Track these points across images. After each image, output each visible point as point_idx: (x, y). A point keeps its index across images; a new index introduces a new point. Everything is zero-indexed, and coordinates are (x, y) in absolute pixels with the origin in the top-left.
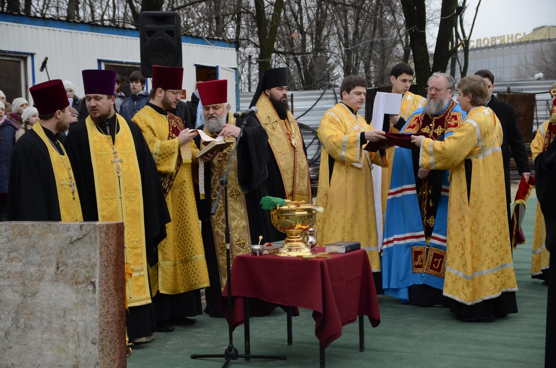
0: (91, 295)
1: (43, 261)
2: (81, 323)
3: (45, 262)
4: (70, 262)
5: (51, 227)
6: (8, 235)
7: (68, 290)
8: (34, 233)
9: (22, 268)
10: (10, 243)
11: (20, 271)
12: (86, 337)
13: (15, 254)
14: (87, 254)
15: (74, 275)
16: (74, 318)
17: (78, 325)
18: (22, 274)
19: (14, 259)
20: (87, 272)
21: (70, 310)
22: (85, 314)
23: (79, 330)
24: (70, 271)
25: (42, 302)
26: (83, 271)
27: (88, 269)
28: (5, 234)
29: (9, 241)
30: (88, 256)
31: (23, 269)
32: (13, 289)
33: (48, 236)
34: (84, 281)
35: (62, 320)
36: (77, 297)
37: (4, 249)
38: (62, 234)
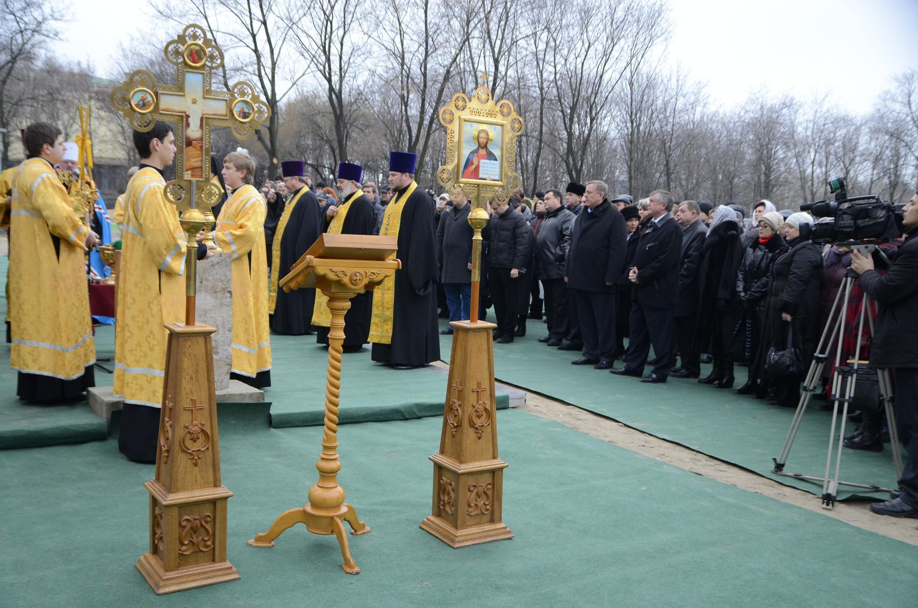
0: (228, 300)
2: (219, 319)
4: (210, 278)
7: (208, 297)
12: (223, 327)
15: (213, 287)
16: (213, 315)
17: (216, 320)
20: (224, 284)
21: (210, 310)
22: (223, 313)
23: (218, 323)
24: (210, 284)
26: (220, 284)
27: (224, 283)
34: (221, 291)
35: (203, 318)
36: (216, 302)
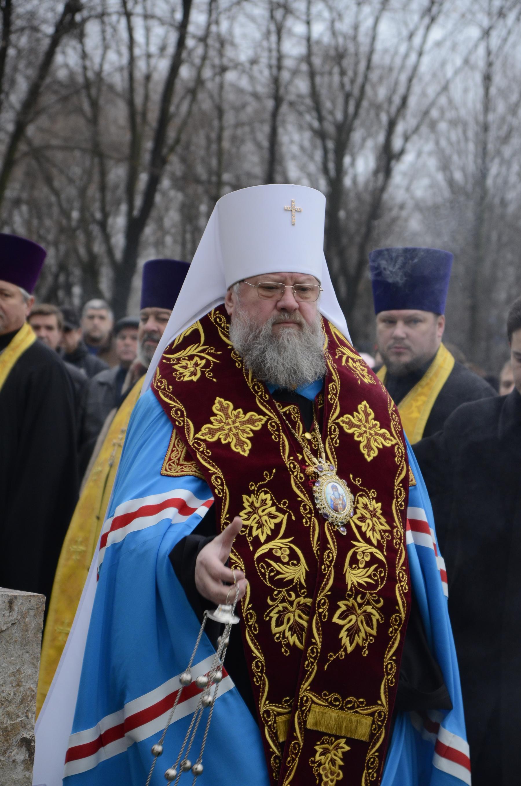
14: (12, 669)
30: (13, 674)
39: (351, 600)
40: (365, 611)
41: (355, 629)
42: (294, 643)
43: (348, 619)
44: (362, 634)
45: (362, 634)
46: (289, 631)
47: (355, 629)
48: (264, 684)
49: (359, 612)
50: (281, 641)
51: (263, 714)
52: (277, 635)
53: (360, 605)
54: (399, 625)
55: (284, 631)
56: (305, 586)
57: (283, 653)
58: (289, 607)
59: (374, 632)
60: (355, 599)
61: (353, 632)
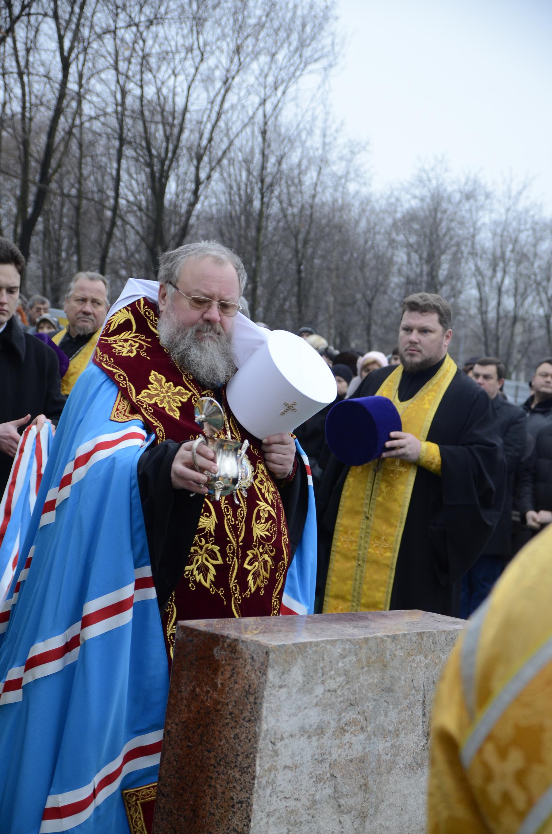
1: (400, 723)
3: (404, 724)
5: (422, 639)
6: (348, 667)
8: (395, 655)
9: (364, 748)
10: (348, 686)
11: (359, 755)
13: (351, 713)
18: (363, 762)
19: (347, 728)
25: (387, 824)
28: (340, 665)
29: (348, 683)
31: (367, 750)
32: (339, 806)
33: (413, 661)
37: (331, 706)
38: (441, 655)
39: (256, 549)
40: (264, 559)
41: (257, 573)
42: (200, 580)
43: (254, 565)
44: (261, 577)
45: (261, 577)
46: (196, 570)
47: (257, 573)
48: (173, 611)
49: (260, 559)
50: (189, 578)
51: (170, 636)
52: (187, 573)
53: (261, 554)
54: (283, 571)
55: (193, 569)
56: (214, 535)
57: (190, 588)
58: (199, 550)
59: (268, 576)
60: (258, 549)
61: (256, 575)
